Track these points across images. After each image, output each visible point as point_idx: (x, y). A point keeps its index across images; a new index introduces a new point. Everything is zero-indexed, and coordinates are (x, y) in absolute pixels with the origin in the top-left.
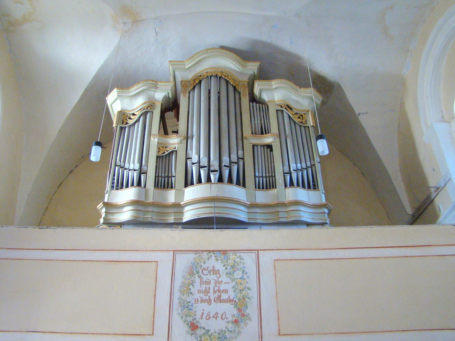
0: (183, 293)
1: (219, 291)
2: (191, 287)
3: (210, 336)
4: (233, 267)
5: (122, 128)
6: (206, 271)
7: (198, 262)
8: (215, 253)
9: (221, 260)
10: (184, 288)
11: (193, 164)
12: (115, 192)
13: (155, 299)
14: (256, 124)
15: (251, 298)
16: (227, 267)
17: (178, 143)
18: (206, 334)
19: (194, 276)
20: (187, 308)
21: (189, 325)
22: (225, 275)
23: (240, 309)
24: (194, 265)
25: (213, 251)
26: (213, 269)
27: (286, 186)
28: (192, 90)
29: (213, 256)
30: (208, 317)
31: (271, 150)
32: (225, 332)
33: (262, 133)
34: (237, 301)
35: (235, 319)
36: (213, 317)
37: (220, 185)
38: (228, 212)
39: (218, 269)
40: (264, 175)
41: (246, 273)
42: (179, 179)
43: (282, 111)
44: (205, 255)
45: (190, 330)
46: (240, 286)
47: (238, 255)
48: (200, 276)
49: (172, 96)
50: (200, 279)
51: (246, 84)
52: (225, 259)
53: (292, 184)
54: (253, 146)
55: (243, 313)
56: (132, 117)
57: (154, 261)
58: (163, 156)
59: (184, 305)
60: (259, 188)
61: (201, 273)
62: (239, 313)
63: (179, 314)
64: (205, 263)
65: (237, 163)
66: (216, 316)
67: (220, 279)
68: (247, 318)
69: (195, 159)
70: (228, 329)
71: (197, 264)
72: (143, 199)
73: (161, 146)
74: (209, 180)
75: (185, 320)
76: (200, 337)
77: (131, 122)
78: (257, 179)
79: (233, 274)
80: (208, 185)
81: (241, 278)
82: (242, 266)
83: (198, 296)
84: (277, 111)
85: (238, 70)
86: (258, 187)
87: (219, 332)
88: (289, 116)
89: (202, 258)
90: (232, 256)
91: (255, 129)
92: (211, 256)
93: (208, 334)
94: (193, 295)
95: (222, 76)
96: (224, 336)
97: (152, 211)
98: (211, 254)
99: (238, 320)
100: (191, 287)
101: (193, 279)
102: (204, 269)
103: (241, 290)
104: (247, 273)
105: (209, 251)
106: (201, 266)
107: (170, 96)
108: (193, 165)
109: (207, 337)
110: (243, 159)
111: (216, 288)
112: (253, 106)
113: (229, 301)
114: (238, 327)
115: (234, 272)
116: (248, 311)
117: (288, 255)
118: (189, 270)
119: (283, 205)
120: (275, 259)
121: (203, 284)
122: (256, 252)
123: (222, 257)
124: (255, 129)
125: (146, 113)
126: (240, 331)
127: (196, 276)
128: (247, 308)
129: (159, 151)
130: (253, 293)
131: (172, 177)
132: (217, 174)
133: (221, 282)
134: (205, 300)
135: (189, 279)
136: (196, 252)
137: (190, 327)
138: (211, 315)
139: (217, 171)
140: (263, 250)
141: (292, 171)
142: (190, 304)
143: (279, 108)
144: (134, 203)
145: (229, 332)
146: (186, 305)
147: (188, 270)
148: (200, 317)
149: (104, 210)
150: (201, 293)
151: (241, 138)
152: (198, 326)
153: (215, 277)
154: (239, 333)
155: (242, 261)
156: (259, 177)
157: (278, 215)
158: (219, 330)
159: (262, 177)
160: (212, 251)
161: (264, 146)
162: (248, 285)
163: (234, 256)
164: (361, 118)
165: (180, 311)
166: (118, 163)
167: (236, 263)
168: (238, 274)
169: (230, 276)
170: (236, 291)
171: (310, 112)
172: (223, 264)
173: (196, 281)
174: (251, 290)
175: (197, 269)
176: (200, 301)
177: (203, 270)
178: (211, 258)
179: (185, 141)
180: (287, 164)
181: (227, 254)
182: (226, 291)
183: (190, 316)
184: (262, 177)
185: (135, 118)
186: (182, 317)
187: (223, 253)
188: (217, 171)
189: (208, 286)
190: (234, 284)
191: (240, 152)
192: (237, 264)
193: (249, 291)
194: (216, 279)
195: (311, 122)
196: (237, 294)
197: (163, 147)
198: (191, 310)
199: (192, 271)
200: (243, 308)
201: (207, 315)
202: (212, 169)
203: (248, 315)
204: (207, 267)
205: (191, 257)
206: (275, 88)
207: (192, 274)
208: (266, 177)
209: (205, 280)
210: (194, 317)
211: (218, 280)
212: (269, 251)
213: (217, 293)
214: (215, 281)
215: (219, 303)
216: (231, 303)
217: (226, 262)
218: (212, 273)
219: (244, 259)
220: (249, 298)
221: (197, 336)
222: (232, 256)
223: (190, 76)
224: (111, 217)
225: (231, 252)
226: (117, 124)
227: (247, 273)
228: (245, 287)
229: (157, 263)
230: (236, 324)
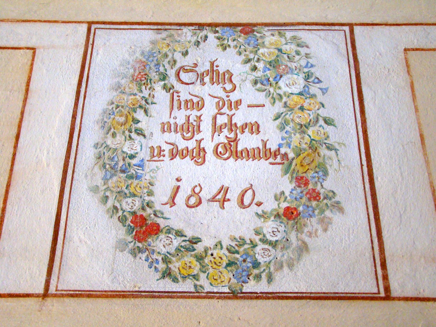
0: (112, 130)
1: (232, 126)
2: (140, 115)
3: (200, 258)
6: (191, 74)
7: (165, 50)
8: (217, 29)
9: (236, 47)
10: (117, 118)
13: (16, 147)
15: (337, 147)
16: (257, 64)
18: (188, 250)
19: (149, 86)
20: (123, 171)
21: (128, 222)
22: (248, 85)
23: (302, 178)
24: (151, 59)
29: (211, 36)
30: (193, 201)
32: (254, 245)
34: (291, 155)
35: (288, 208)
36: (213, 199)
39: (228, 71)
41: (316, 81)
45: (130, 239)
46: (300, 114)
47: (289, 35)
48: (169, 86)
50: (169, 95)
52: (249, 44)
55: (314, 190)
57: (23, 45)
59: (113, 163)
61: (172, 80)
62: (299, 190)
63: (95, 189)
64: (185, 54)
67: (234, 97)
68: (326, 204)
70: (264, 236)
71: (159, 56)
75: (115, 208)
76: (166, 260)
79: (277, 83)
81: (301, 94)
82: (303, 63)
87: (233, 244)
89: (176, 41)
92: (206, 37)
93: (194, 250)
94: (144, 136)
96: (249, 260)
98: (204, 33)
99: (295, 209)
100: (140, 115)
101: (146, 93)
102: (182, 68)
103: (301, 126)
104: (320, 81)
105: (201, 26)
106: (175, 62)
111: (222, 120)
114: (299, 230)
115: (279, 77)
118: (135, 70)
120: (407, 48)
121: (179, 108)
122: (347, 28)
123: (241, 40)
126: (304, 243)
128: (326, 173)
133: (238, 103)
134: (185, 152)
135: (135, 95)
136: (159, 27)
137: (130, 230)
138: (205, 195)
140: (368, 24)
142: (134, 161)
145: (266, 246)
146: (121, 163)
147: (132, 71)
148: (165, 199)
150: (171, 131)
152: (158, 226)
155: (303, 51)
158: (234, 239)
160: (210, 25)
162: (323, 112)
163: (276, 38)
165: (100, 182)
167: (285, 56)
169: (266, 87)
170: (288, 128)
172: (243, 57)
173: (155, 100)
174: (334, 125)
175: (162, 69)
176: (166, 153)
177: (179, 72)
178: (206, 42)
181: (255, 33)
183: (134, 195)
187: (241, 32)
189: (194, 113)
190: (279, 107)
192: (288, 57)
193: (329, 129)
194: (223, 95)
196: (290, 137)
198: (138, 177)
199: (146, 75)
200: (311, 174)
201: (189, 192)
203: (331, 194)
204: (193, 65)
207: (143, 82)
209: (184, 96)
210: (147, 198)
211: (226, 99)
212: (387, 27)
213: (225, 131)
214: (217, 100)
215: (232, 159)
216: (271, 160)
217: (251, 52)
218: (207, 79)
219: (307, 47)
220: (330, 148)
221: (155, 256)
225: (266, 28)
227: (320, 81)
228: (317, 118)
229: (32, 51)
230: (291, 222)
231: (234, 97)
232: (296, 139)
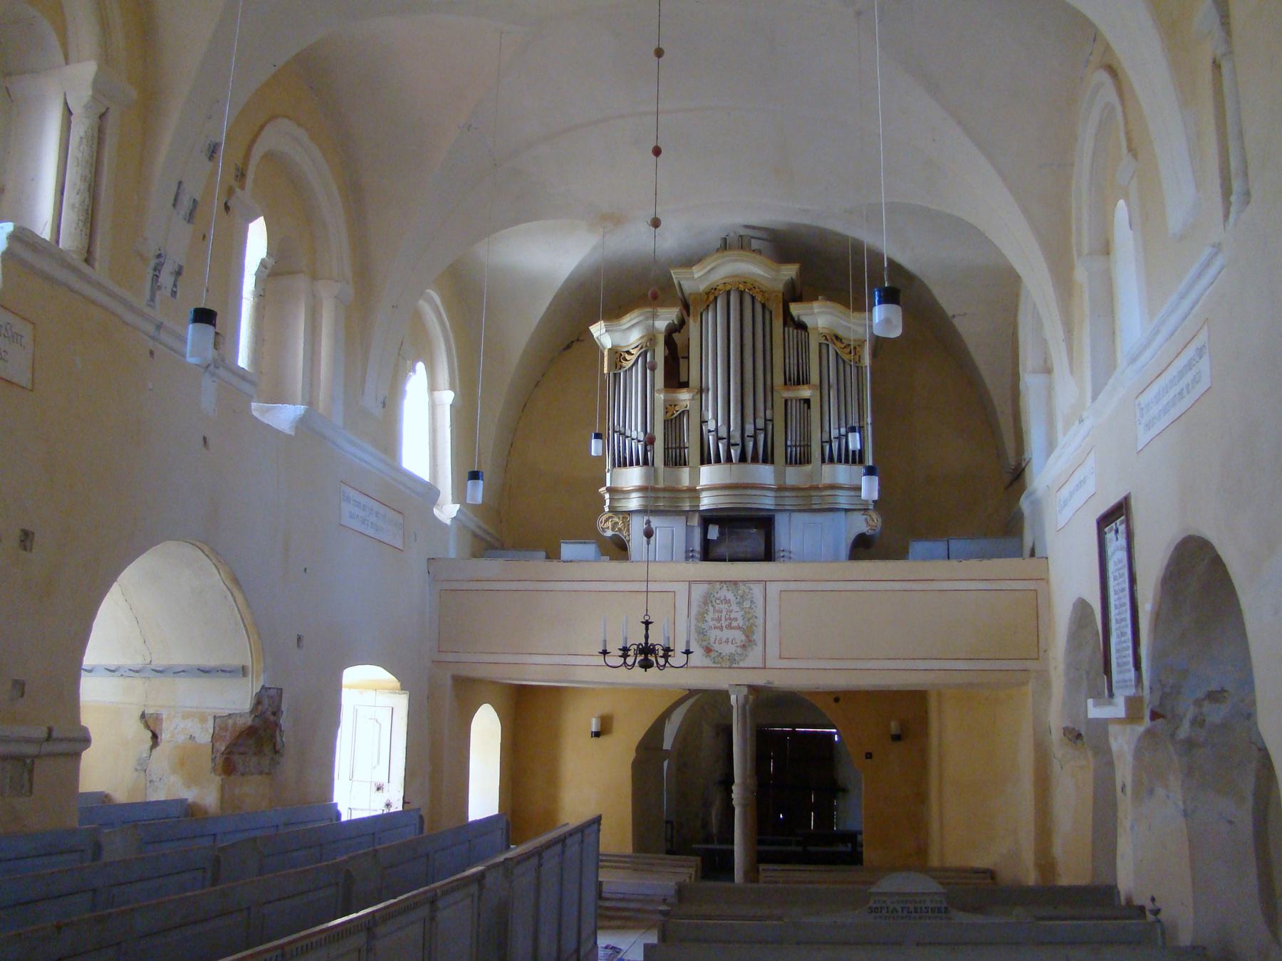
1: (730, 619)
2: (705, 615)
3: (722, 658)
4: (742, 597)
5: (615, 374)
11: (710, 431)
12: (617, 470)
17: (689, 400)
22: (735, 605)
25: (725, 581)
26: (725, 599)
27: (823, 461)
28: (704, 310)
29: (725, 586)
31: (809, 407)
33: (799, 384)
37: (743, 465)
38: (751, 501)
40: (798, 444)
42: (693, 453)
43: (828, 345)
44: (718, 586)
47: (747, 585)
49: (678, 321)
51: (781, 295)
53: (831, 460)
54: (786, 401)
56: (628, 357)
58: (672, 420)
60: (791, 463)
63: (696, 639)
64: (717, 593)
65: (765, 429)
66: (727, 641)
67: (731, 608)
69: (712, 426)
72: (652, 484)
73: (670, 405)
74: (729, 459)
77: (627, 365)
78: (789, 450)
80: (728, 466)
83: (711, 623)
84: (820, 344)
85: (766, 275)
86: (790, 461)
88: (837, 353)
90: (742, 587)
97: (664, 498)
105: (722, 582)
107: (676, 322)
108: (710, 434)
109: (719, 659)
110: (772, 420)
111: (727, 616)
113: (739, 628)
116: (754, 637)
117: (793, 586)
119: (816, 488)
125: (645, 353)
127: (710, 607)
129: (667, 412)
130: (760, 622)
131: (685, 448)
132: (739, 449)
133: (732, 610)
139: (738, 445)
141: (832, 437)
144: (642, 489)
148: (713, 641)
149: (607, 496)
151: (769, 390)
153: (726, 606)
154: (747, 655)
155: (751, 592)
156: (791, 446)
157: (811, 500)
159: (796, 446)
161: (800, 400)
162: (755, 614)
164: (956, 322)
166: (617, 429)
168: (747, 604)
179: (699, 395)
180: (828, 430)
182: (736, 619)
184: (796, 446)
185: (632, 359)
186: (698, 642)
188: (738, 445)
190: (743, 612)
191: (769, 413)
193: (756, 620)
197: (671, 405)
202: (732, 441)
205: (705, 587)
206: (818, 313)
208: (800, 446)
213: (728, 621)
220: (756, 626)
222: (742, 587)
223: (702, 287)
224: (616, 504)
226: (609, 370)
231: (731, 608)
232: (747, 623)
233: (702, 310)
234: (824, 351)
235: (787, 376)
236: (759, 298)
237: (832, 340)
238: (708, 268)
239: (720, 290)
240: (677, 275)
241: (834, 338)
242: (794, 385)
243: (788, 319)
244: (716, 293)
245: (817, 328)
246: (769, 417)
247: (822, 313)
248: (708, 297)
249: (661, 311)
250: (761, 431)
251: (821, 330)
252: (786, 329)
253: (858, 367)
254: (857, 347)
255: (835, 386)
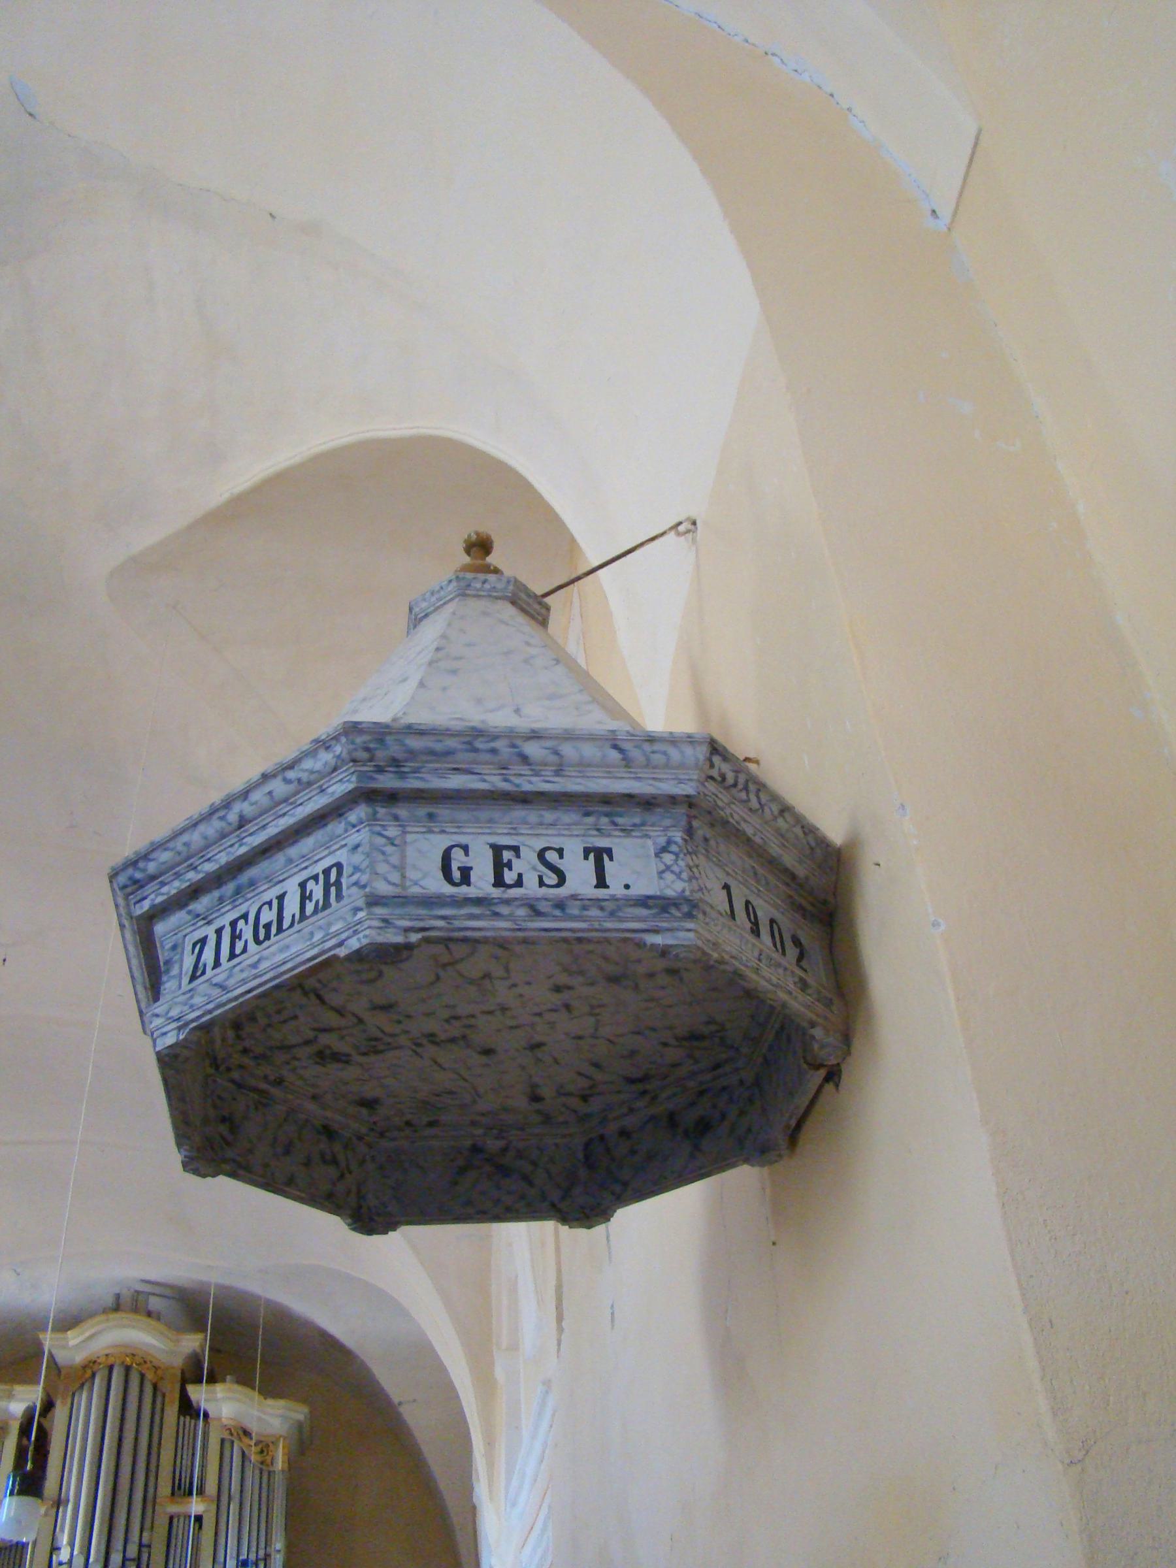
14: (184, 1468)
43: (232, 1442)
54: (171, 1518)
84: (223, 1441)
85: (164, 1347)
88: (243, 1453)
91: (180, 1480)
95: (132, 1364)
112: (184, 1422)
124: (180, 1480)
143: (226, 1435)
164: (407, 1412)
171: (282, 1439)
191: (145, 1534)
195: (280, 1464)
223: (79, 1358)
233: (74, 1389)
234: (227, 1445)
235: (177, 1482)
236: (150, 1376)
237: (238, 1434)
238: (87, 1334)
239: (100, 1364)
240: (48, 1340)
241: (241, 1433)
242: (184, 1495)
243: (187, 1408)
244: (95, 1367)
245: (219, 1419)
246: (145, 1541)
247: (229, 1398)
248: (85, 1371)
249: (19, 1389)
250: (132, 1563)
251: (224, 1421)
252: (182, 1418)
253: (269, 1472)
254: (271, 1445)
255: (238, 1496)
